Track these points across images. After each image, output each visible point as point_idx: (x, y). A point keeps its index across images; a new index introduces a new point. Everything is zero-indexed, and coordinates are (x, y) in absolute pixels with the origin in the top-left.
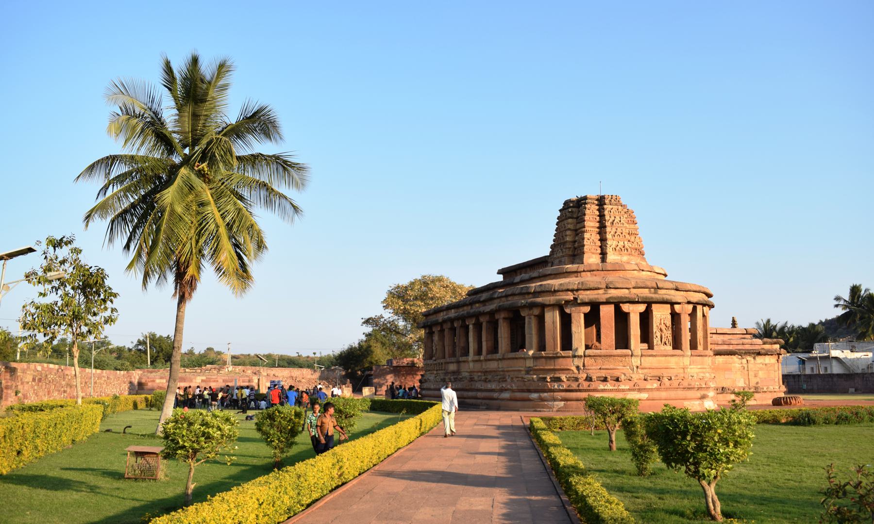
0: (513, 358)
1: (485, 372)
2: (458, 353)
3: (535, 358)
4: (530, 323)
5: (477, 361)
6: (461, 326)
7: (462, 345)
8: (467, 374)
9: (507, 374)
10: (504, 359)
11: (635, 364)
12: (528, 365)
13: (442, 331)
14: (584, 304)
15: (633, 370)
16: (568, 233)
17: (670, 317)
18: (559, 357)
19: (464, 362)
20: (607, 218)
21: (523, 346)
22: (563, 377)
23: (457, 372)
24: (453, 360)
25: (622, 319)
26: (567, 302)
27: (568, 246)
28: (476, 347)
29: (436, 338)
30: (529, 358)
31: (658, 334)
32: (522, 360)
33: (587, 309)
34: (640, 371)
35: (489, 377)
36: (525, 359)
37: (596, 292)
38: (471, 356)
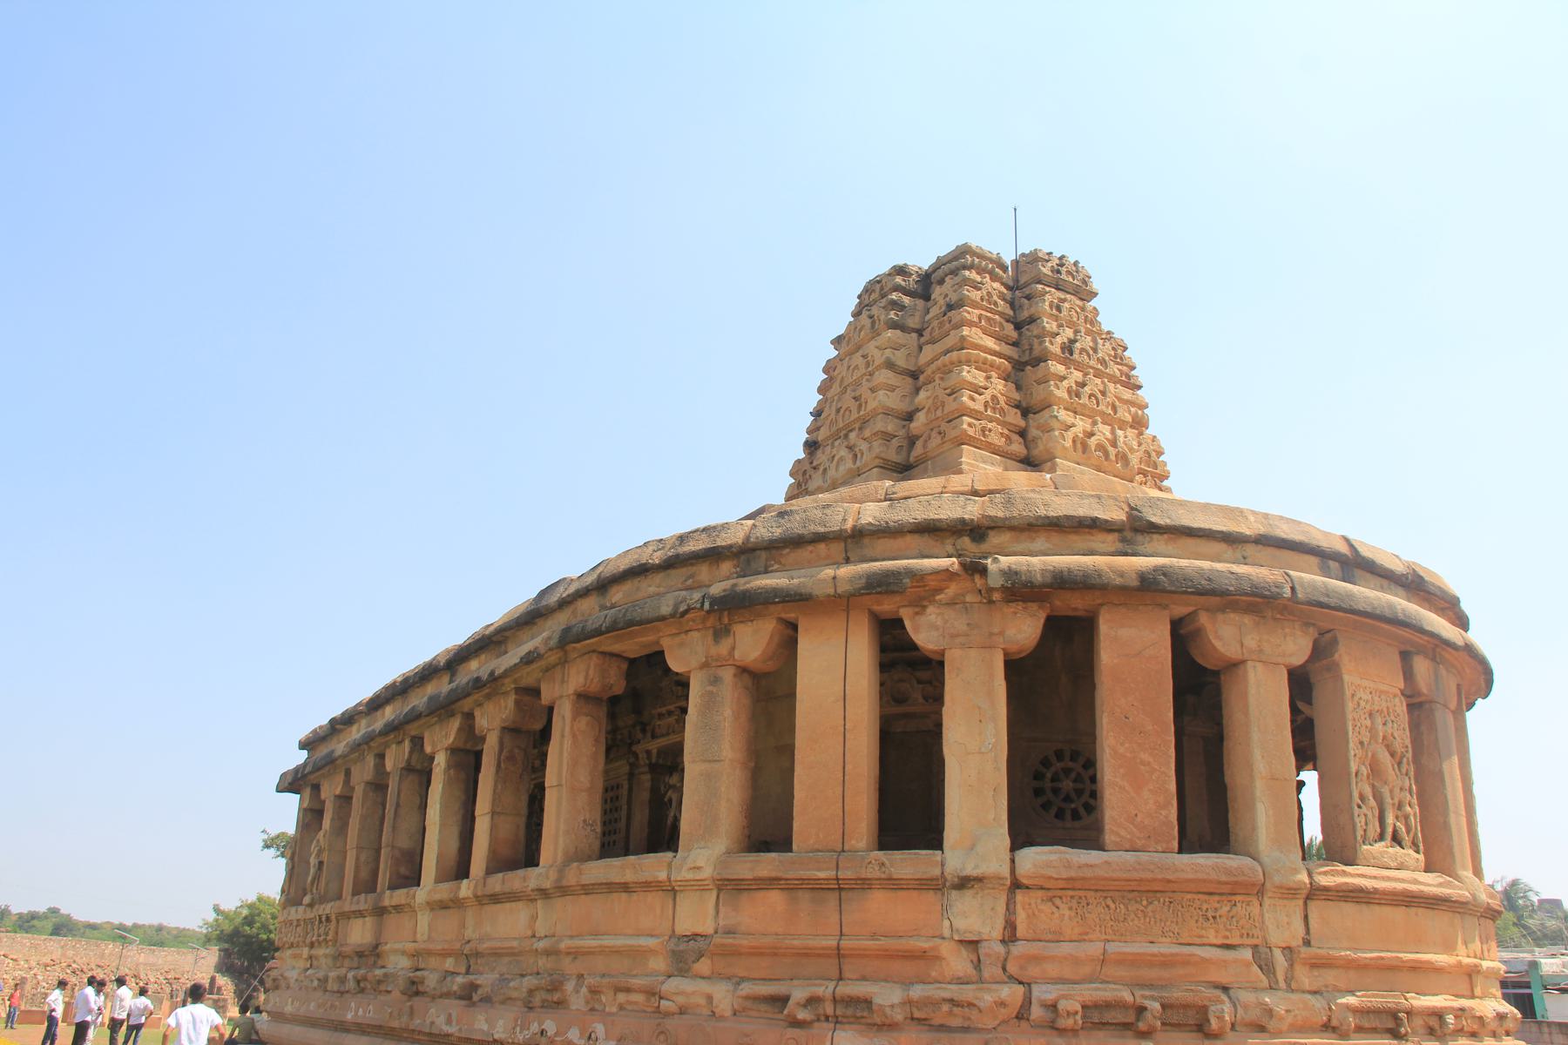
0: (611, 887)
1: (471, 957)
2: (384, 878)
3: (730, 887)
4: (710, 702)
5: (443, 906)
6: (409, 769)
7: (404, 842)
8: (405, 962)
9: (569, 967)
10: (563, 890)
11: (1277, 937)
12: (685, 926)
13: (345, 799)
14: (1019, 591)
15: (1267, 967)
16: (885, 376)
17: (1401, 707)
18: (864, 885)
19: (398, 908)
20: (1050, 325)
21: (663, 835)
22: (887, 996)
23: (372, 954)
24: (364, 902)
25: (1199, 691)
26: (924, 589)
27: (880, 424)
28: (454, 845)
29: (327, 822)
30: (699, 886)
31: (1368, 791)
32: (654, 899)
33: (1024, 629)
34: (1304, 978)
35: (486, 980)
36: (671, 890)
37: (1078, 541)
38: (429, 887)
